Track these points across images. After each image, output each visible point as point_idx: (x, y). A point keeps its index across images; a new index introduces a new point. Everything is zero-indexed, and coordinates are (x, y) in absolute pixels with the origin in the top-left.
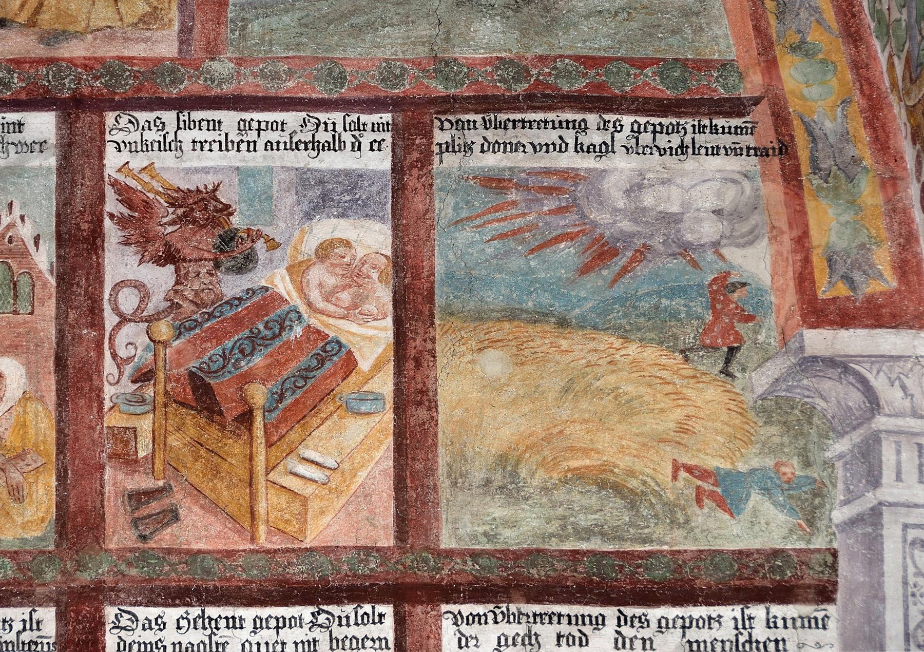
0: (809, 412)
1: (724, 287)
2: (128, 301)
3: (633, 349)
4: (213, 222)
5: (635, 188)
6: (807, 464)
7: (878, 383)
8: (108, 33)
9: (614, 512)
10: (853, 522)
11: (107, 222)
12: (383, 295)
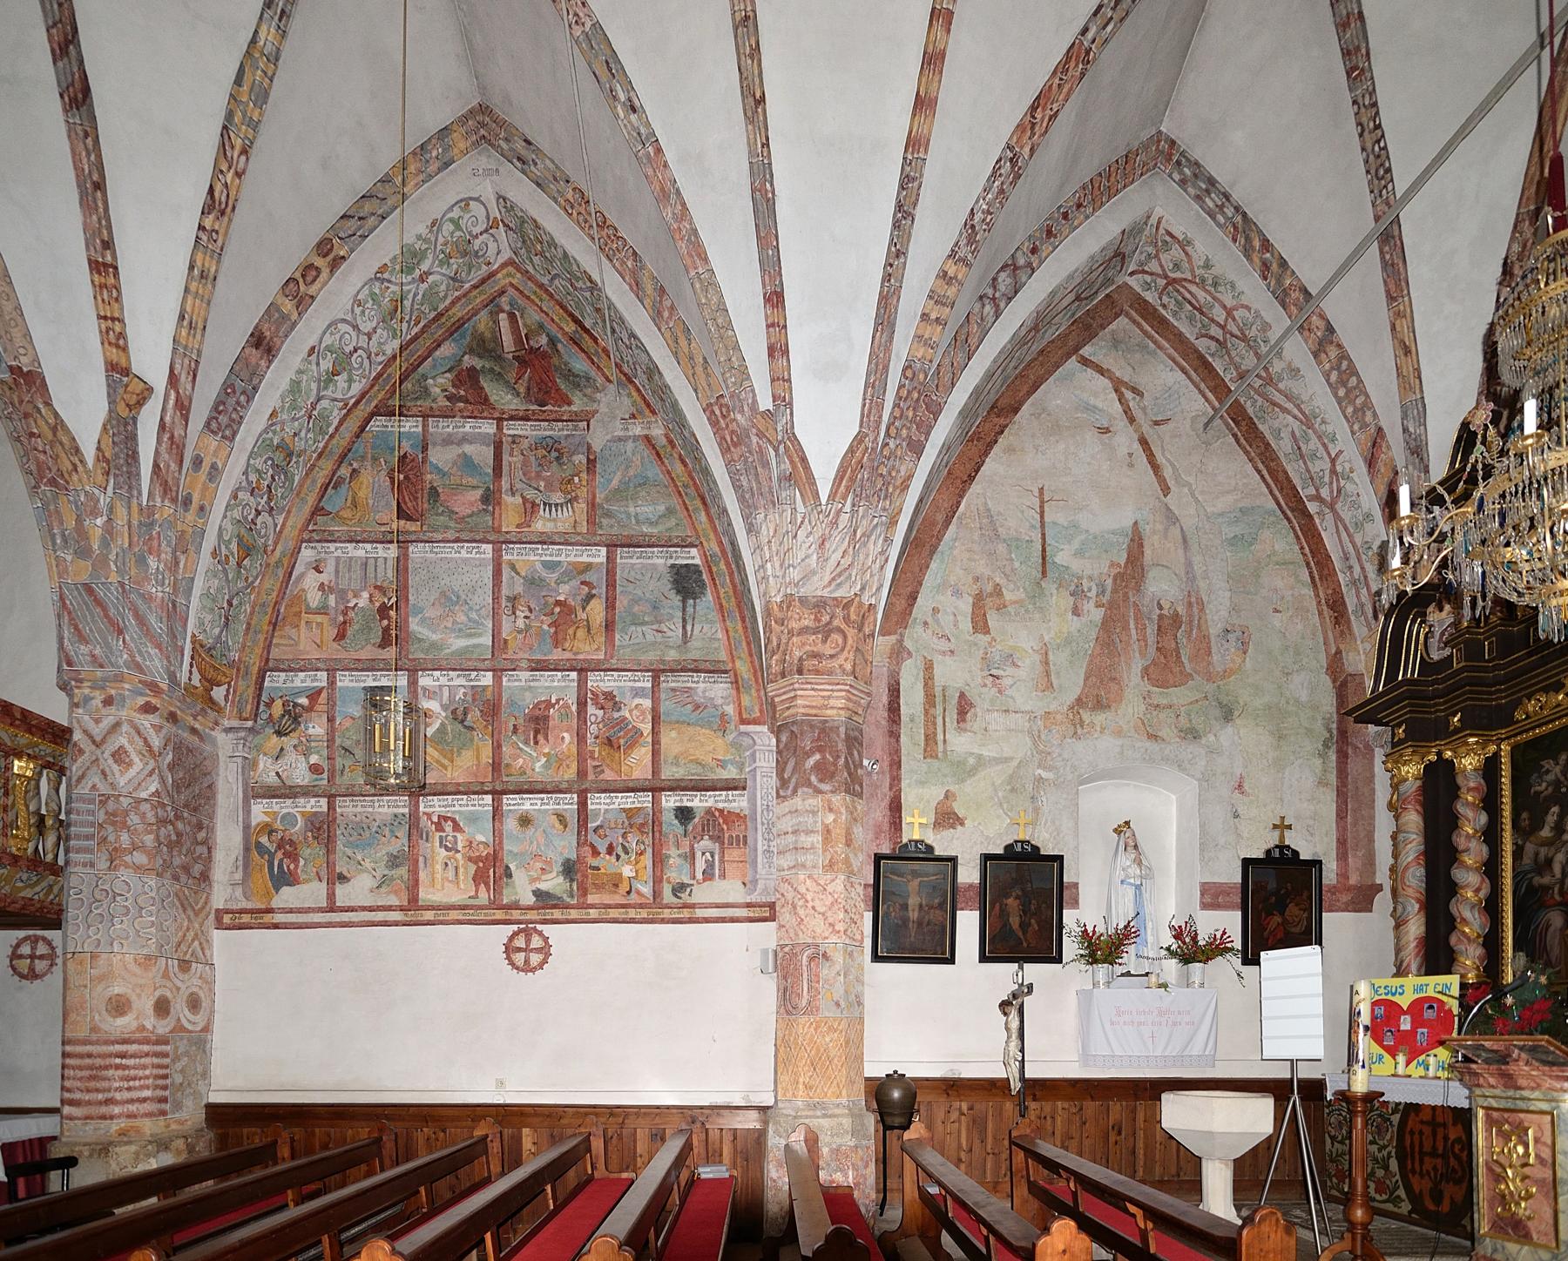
1: (723, 715)
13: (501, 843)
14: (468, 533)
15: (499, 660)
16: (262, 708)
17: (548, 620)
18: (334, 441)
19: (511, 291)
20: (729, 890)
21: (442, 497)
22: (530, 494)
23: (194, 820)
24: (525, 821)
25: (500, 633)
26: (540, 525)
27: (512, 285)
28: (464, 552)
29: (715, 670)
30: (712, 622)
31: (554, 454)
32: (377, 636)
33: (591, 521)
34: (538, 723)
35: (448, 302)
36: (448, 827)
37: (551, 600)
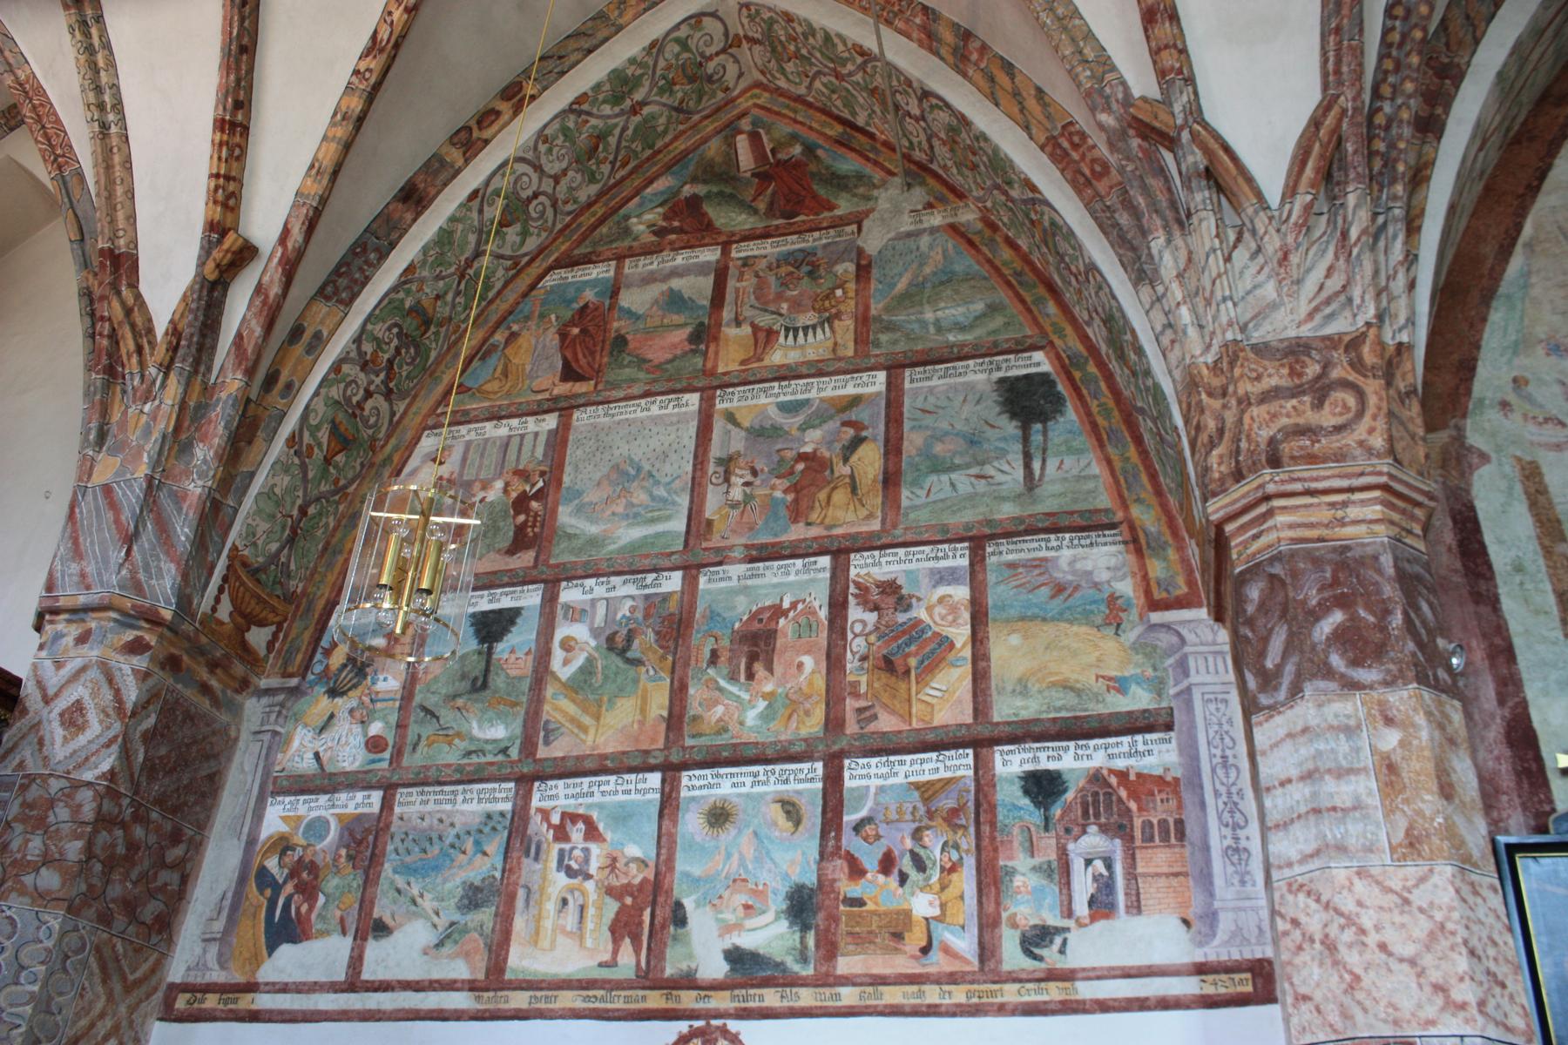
0: (1155, 647)
1: (1112, 599)
2: (858, 628)
3: (1075, 628)
4: (894, 593)
5: (1072, 563)
6: (1155, 669)
7: (1184, 632)
8: (852, 523)
9: (1071, 699)
10: (1178, 694)
11: (850, 598)
12: (966, 616)
13: (670, 860)
14: (667, 383)
15: (697, 552)
16: (318, 656)
17: (786, 483)
18: (493, 307)
19: (755, 111)
20: (1154, 936)
21: (631, 346)
22: (764, 320)
23: (168, 827)
24: (719, 816)
25: (701, 511)
26: (777, 357)
27: (756, 105)
28: (656, 408)
29: (1088, 524)
30: (1080, 452)
31: (806, 269)
32: (507, 536)
33: (861, 340)
34: (757, 644)
35: (668, 139)
36: (577, 832)
37: (789, 454)
